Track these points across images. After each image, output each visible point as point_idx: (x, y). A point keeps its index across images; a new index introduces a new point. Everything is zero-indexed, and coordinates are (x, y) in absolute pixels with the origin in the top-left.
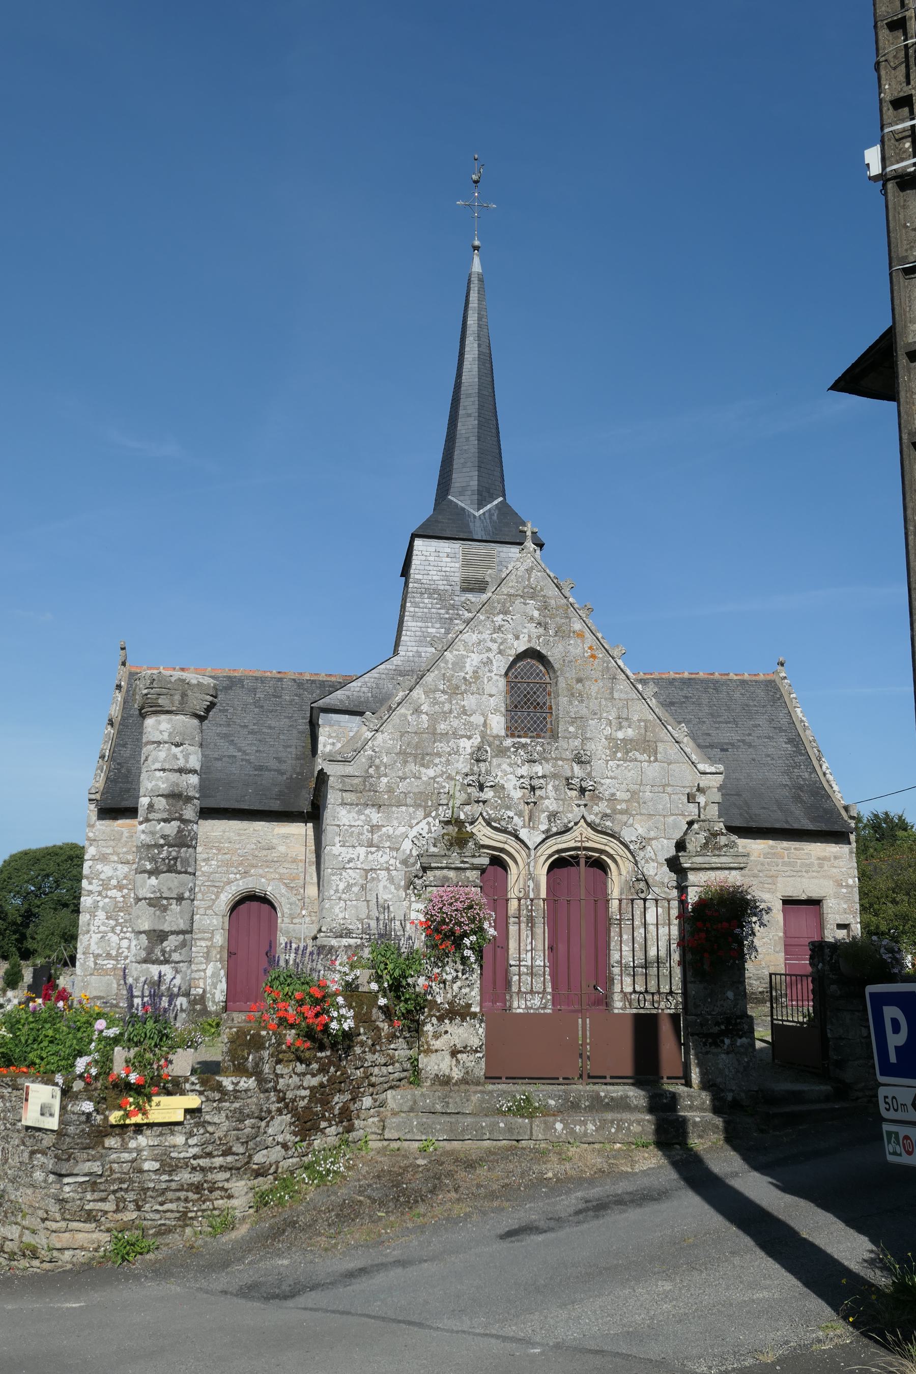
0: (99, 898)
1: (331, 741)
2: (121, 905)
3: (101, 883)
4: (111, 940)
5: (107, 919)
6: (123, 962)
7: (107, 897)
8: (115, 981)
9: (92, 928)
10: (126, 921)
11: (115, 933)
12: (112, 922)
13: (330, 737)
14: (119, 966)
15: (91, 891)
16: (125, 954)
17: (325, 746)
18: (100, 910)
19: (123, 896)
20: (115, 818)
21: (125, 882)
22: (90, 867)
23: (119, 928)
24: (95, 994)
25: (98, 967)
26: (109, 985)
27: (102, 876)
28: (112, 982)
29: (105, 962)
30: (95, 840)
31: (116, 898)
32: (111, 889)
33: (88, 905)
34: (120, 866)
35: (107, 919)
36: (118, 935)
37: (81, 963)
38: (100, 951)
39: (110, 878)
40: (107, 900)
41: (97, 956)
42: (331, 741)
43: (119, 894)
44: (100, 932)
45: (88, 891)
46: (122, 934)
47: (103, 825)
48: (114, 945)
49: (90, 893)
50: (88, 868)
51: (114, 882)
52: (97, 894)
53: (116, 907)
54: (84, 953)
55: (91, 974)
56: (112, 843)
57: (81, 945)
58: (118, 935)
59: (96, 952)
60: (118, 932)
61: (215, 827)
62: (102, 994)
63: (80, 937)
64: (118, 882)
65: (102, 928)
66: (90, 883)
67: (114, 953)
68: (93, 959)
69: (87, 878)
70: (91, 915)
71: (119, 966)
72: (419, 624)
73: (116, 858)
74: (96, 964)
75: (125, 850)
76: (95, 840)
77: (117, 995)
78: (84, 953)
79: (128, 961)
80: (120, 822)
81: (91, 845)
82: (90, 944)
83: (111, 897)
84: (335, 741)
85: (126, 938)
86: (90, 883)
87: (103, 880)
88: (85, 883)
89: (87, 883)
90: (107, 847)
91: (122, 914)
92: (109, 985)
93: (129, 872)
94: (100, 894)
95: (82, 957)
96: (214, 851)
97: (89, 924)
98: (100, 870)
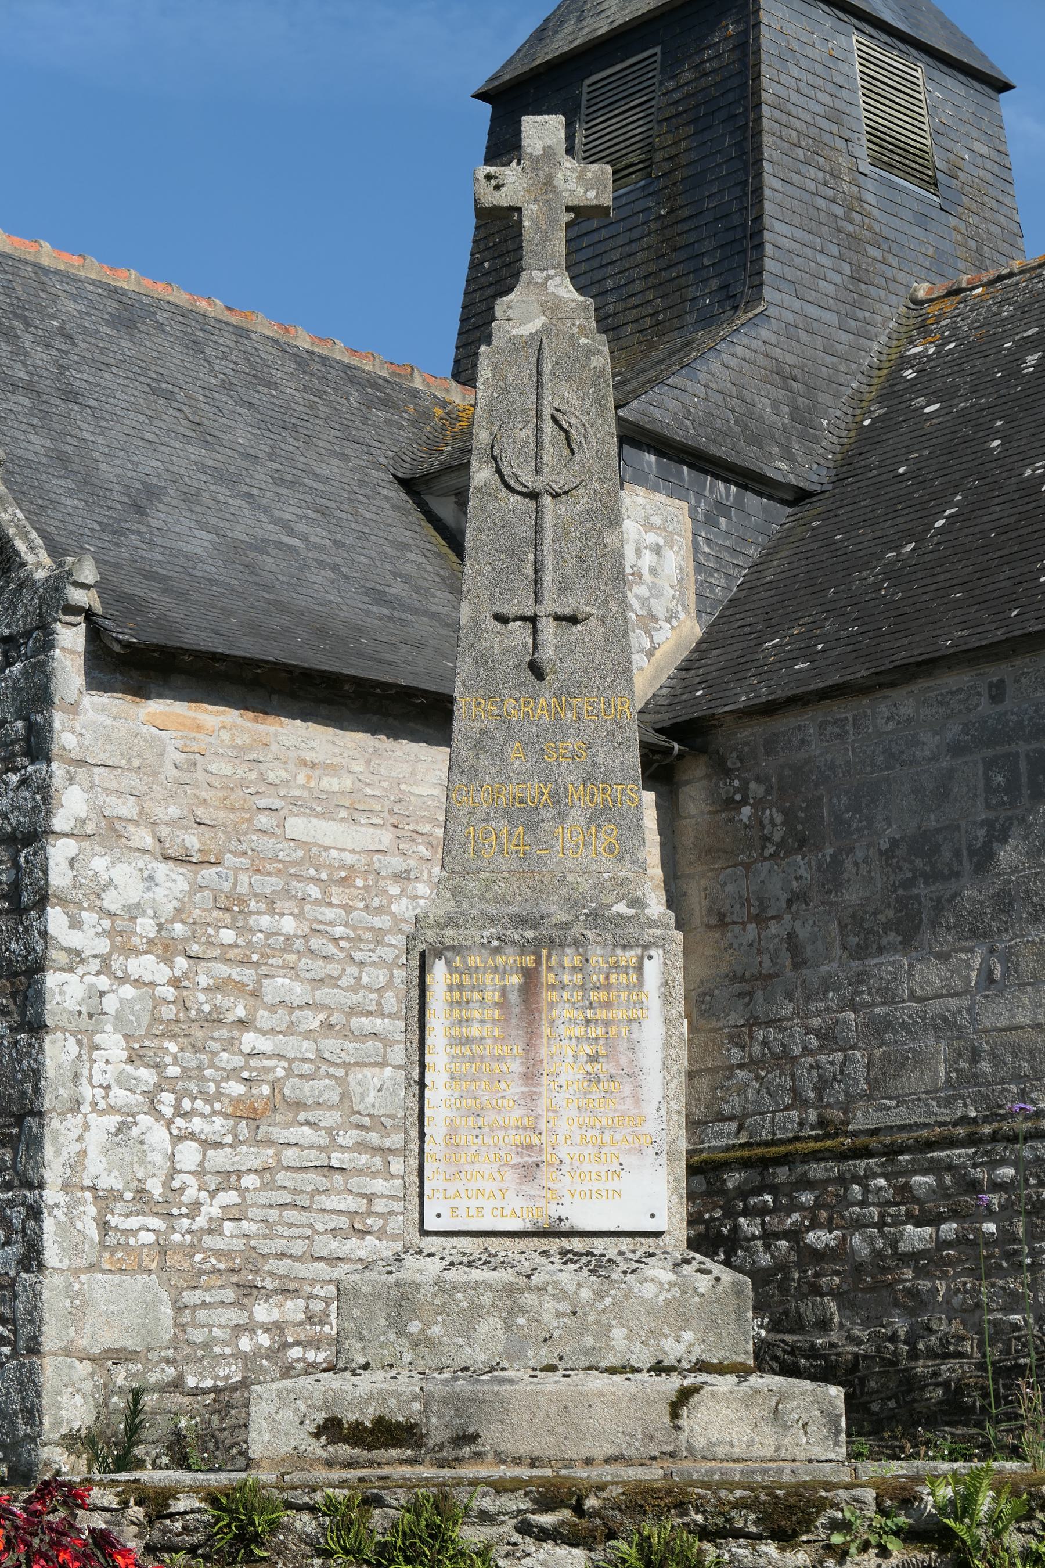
0: (103, 982)
1: (651, 538)
2: (169, 1012)
3: (106, 924)
4: (149, 1139)
5: (130, 1060)
6: (185, 1222)
7: (123, 980)
8: (165, 1295)
9: (87, 1092)
10: (186, 1075)
11: (159, 1115)
12: (147, 1076)
13: (649, 526)
14: (177, 1237)
15: (78, 953)
16: (191, 1193)
17: (638, 552)
18: (109, 1028)
19: (175, 982)
20: (141, 692)
21: (179, 928)
22: (72, 863)
23: (168, 1097)
24: (110, 1339)
25: (111, 1239)
26: (150, 1307)
27: (111, 901)
28: (156, 1302)
29: (134, 1222)
30: (81, 763)
31: (153, 984)
32: (136, 952)
33: (71, 1005)
34: (162, 869)
35: (130, 1060)
36: (169, 1124)
37: (58, 1223)
38: (110, 1181)
39: (134, 911)
40: (128, 991)
41: (106, 1199)
42: (651, 538)
43: (162, 973)
44: (111, 1109)
45: (68, 950)
46: (179, 1122)
47: (103, 709)
48: (158, 1158)
49: (76, 955)
50: (65, 865)
51: (146, 926)
52: (95, 965)
53: (155, 1020)
54: (66, 1187)
55: (92, 1267)
56: (132, 781)
57: (57, 1153)
58: (169, 1124)
59: (104, 1183)
60: (168, 1112)
61: (421, 767)
62: (130, 1343)
63: (53, 1123)
64: (160, 926)
65: (119, 1096)
66: (75, 924)
67: (155, 1188)
68: (92, 1211)
69: (63, 902)
70: (79, 1043)
71: (177, 1237)
72: (799, 234)
73: (149, 841)
74: (105, 1227)
75: (174, 811)
76: (81, 763)
77: (174, 1344)
78: (66, 1187)
79: (201, 1222)
80: (156, 707)
81: (71, 779)
82: (83, 1153)
83: (138, 982)
84: (661, 542)
85: (191, 1136)
86: (75, 924)
87: (111, 915)
88: (56, 919)
89: (64, 920)
90: (120, 793)
91: (173, 1048)
92: (150, 1307)
93: (191, 893)
94: (106, 968)
95: (61, 1198)
96: (422, 849)
97: (76, 1077)
98: (104, 877)
